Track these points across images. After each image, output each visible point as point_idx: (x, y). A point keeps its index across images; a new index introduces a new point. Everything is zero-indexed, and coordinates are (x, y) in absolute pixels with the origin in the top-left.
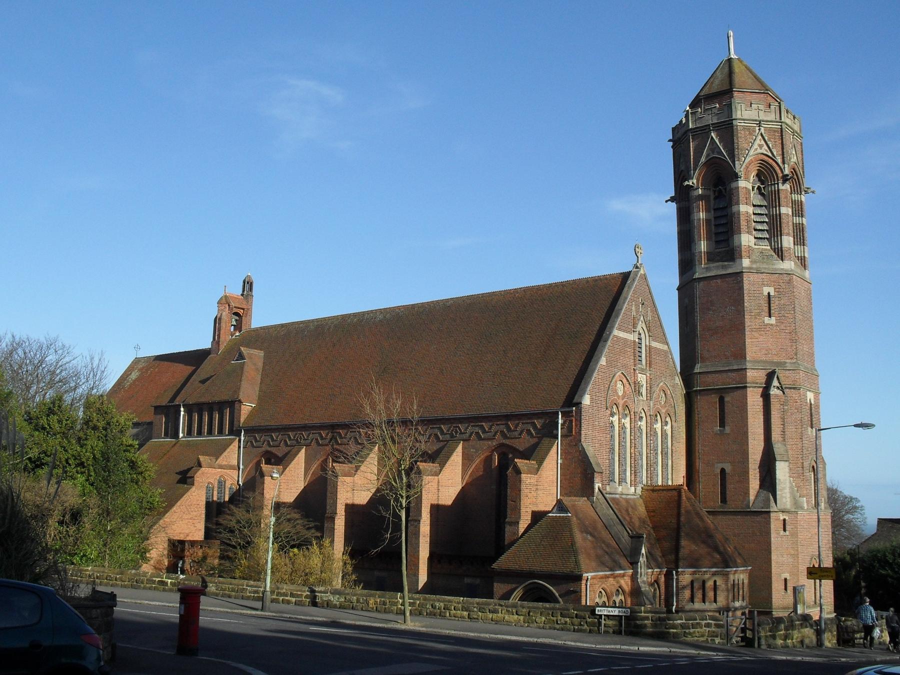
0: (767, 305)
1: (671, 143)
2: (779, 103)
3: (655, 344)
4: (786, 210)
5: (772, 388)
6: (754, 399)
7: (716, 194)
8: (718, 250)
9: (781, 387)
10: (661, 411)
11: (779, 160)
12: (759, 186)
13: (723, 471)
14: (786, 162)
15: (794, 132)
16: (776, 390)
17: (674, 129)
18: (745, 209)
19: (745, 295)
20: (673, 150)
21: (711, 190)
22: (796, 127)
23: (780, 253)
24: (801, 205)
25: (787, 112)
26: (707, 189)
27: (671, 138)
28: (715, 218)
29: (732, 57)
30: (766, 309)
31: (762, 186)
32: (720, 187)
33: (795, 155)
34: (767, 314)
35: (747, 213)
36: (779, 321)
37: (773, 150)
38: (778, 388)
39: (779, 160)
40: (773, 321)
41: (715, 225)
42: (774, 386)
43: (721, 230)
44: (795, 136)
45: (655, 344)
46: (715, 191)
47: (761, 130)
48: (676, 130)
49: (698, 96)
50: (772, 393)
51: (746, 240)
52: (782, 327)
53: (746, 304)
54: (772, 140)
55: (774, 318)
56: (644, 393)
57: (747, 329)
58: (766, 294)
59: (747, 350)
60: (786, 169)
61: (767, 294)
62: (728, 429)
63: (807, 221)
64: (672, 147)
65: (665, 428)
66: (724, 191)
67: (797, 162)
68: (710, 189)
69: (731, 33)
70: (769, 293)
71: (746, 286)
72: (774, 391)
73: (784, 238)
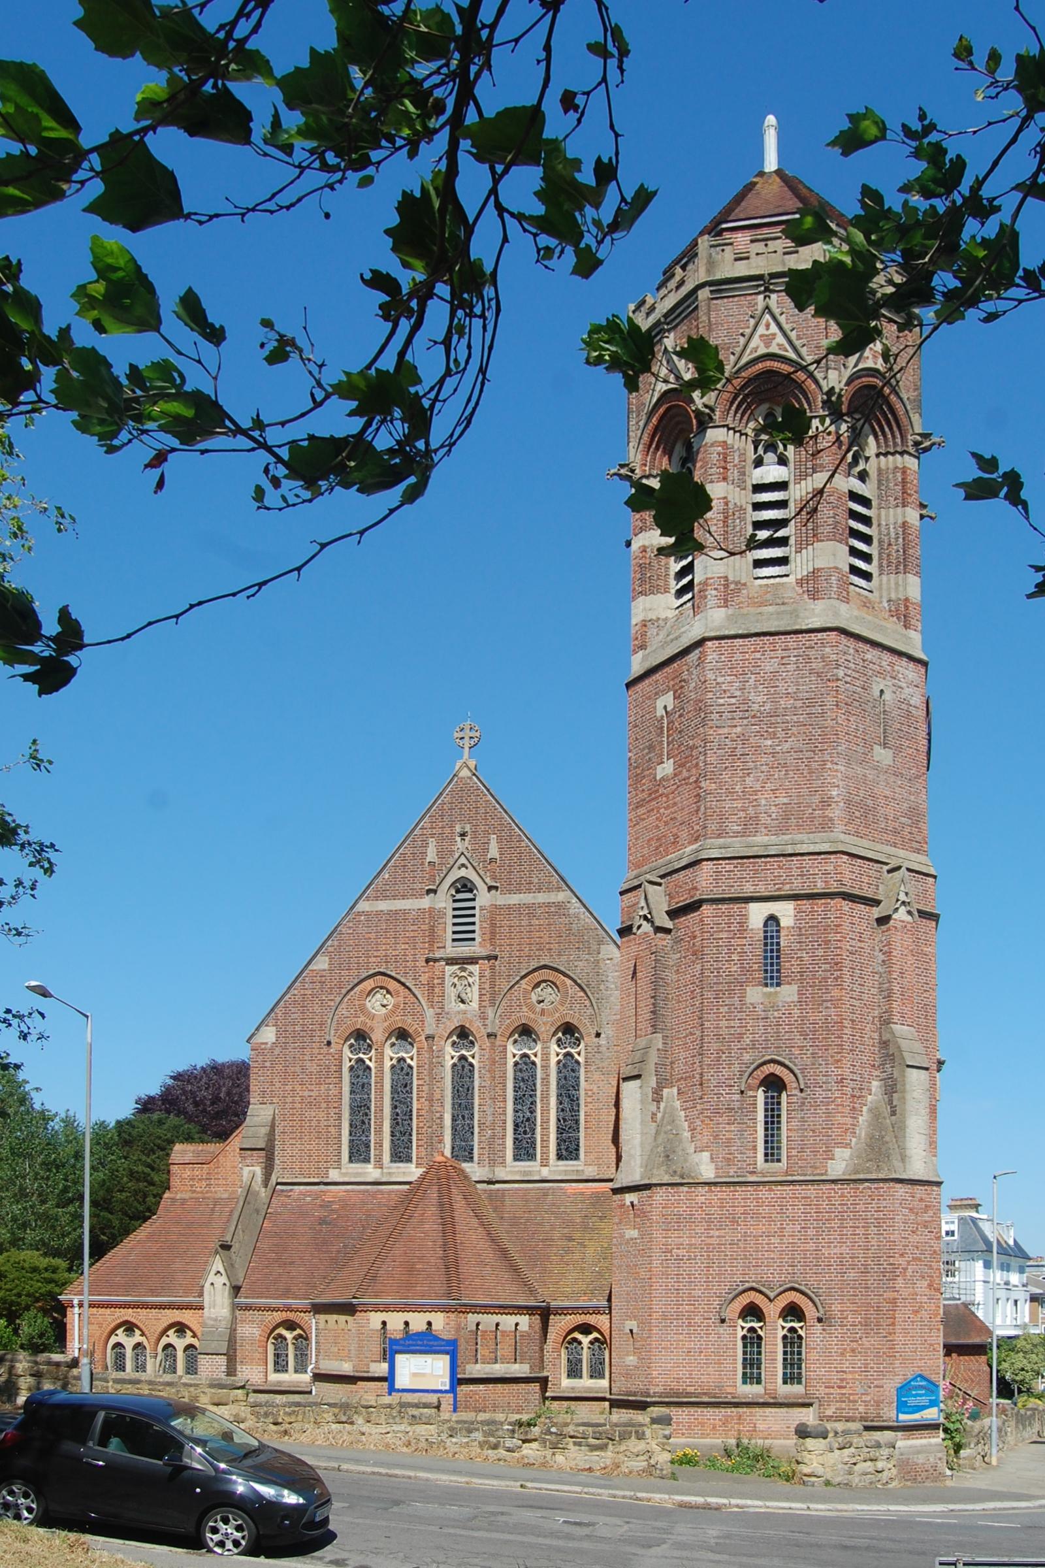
52: (685, 774)
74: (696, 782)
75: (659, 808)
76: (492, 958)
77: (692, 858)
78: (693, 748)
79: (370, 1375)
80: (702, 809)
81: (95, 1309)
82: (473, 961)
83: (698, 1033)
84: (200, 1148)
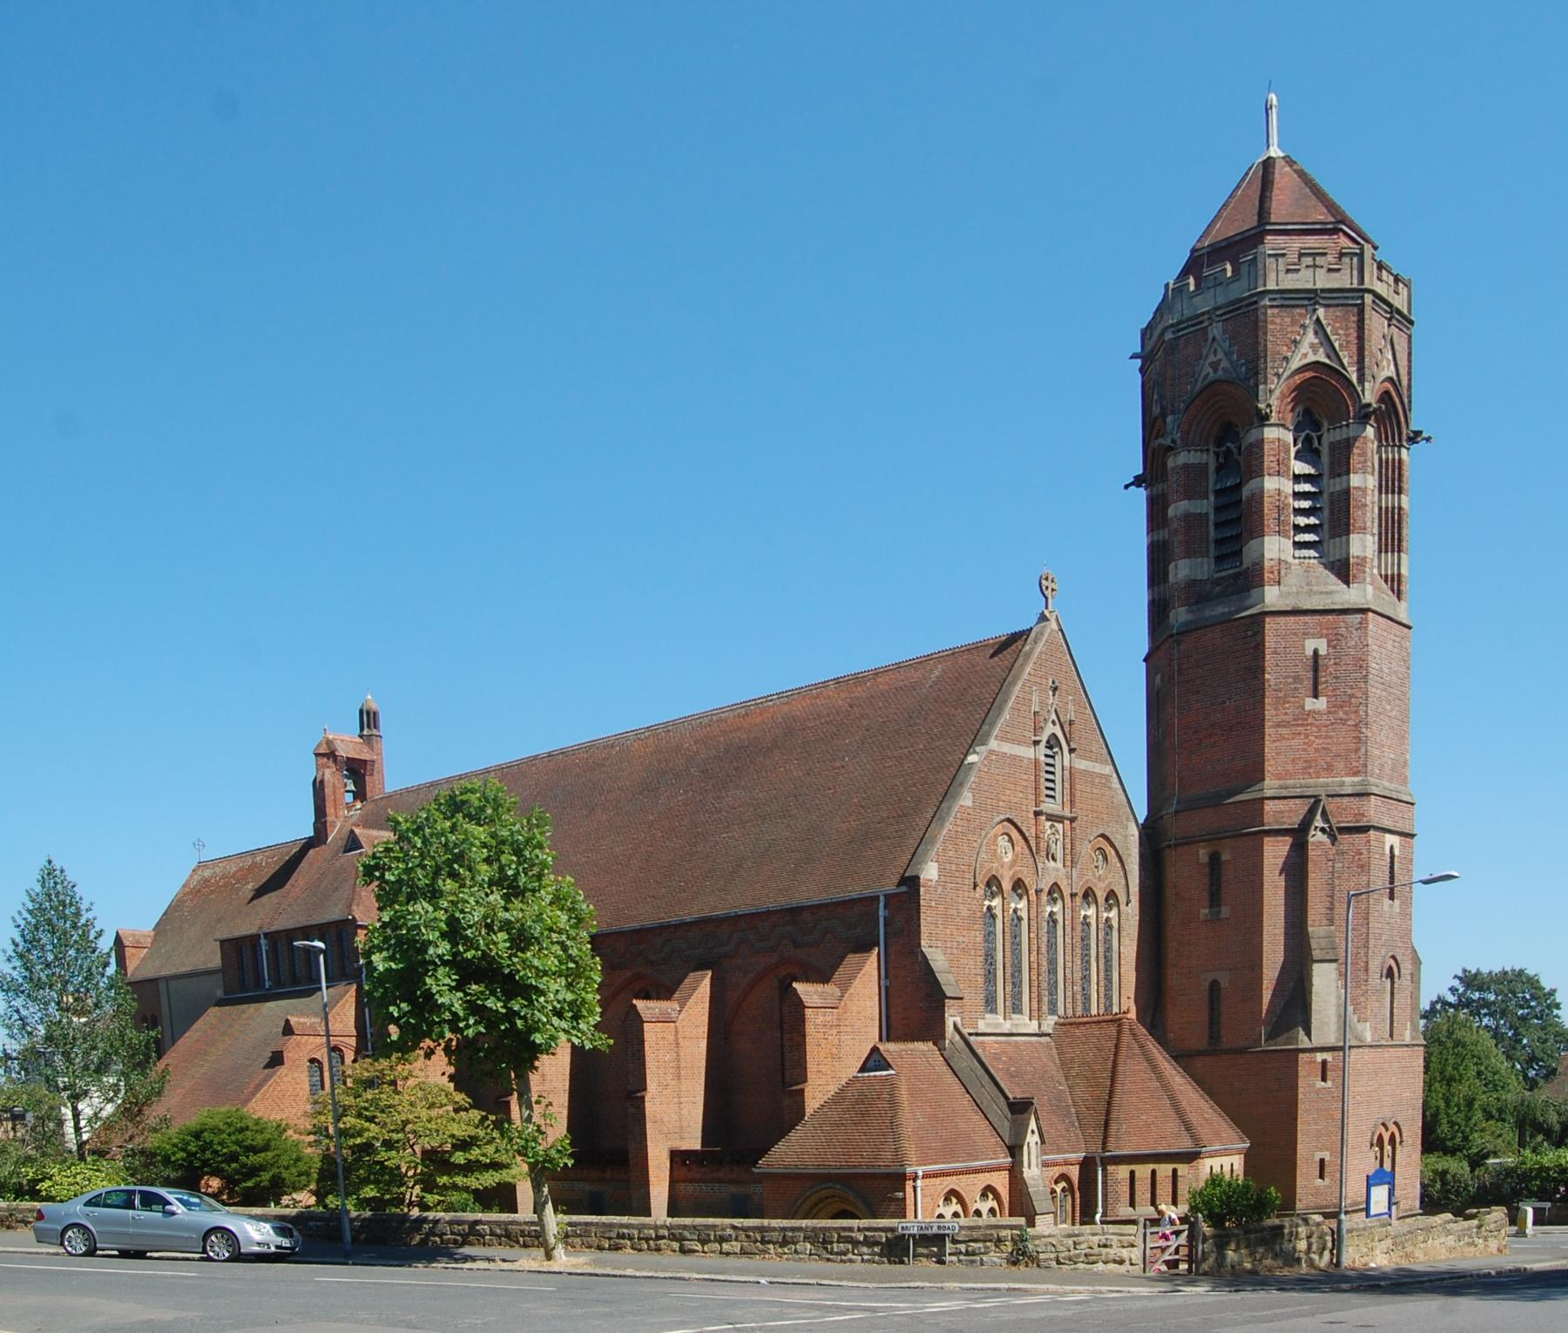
0: (1310, 675)
1: (1139, 362)
2: (1362, 249)
3: (1081, 765)
4: (1364, 481)
5: (1313, 832)
6: (1275, 852)
7: (1221, 460)
8: (1219, 575)
9: (1330, 827)
10: (1095, 885)
11: (1354, 378)
12: (1308, 434)
13: (1214, 986)
14: (1368, 376)
15: (1393, 313)
16: (1319, 833)
17: (1144, 333)
18: (1273, 485)
19: (1267, 657)
20: (1143, 376)
21: (1211, 452)
22: (1399, 302)
23: (1343, 570)
24: (1400, 468)
25: (1380, 267)
26: (1202, 451)
27: (1139, 350)
28: (1218, 509)
29: (1273, 154)
30: (1308, 684)
31: (1313, 434)
32: (1229, 444)
33: (1392, 363)
34: (1310, 692)
35: (1279, 492)
36: (1334, 707)
37: (1341, 354)
38: (1323, 830)
39: (1354, 378)
40: (1321, 704)
41: (1217, 525)
42: (1316, 827)
43: (1228, 533)
44: (1394, 322)
45: (1081, 765)
46: (1217, 455)
47: (1318, 312)
48: (1148, 332)
49: (1193, 251)
50: (1311, 840)
51: (1275, 548)
52: (1341, 715)
53: (1267, 676)
54: (1341, 332)
55: (1325, 698)
56: (1059, 856)
57: (1267, 724)
58: (1310, 652)
59: (1266, 763)
60: (1366, 393)
61: (1311, 653)
62: (1225, 911)
63: (1410, 502)
64: (1141, 370)
65: (1105, 915)
66: (1235, 450)
67: (1395, 378)
68: (1208, 450)
69: (1273, 97)
70: (1316, 652)
71: (1270, 641)
72: (1316, 837)
73: (1355, 539)
74: (1356, 725)
75: (1307, 736)
76: (1072, 820)
77: (1358, 789)
78: (1352, 696)
79: (1119, 1218)
80: (1363, 750)
81: (928, 1180)
82: (1060, 819)
83: (1364, 930)
84: (820, 990)
